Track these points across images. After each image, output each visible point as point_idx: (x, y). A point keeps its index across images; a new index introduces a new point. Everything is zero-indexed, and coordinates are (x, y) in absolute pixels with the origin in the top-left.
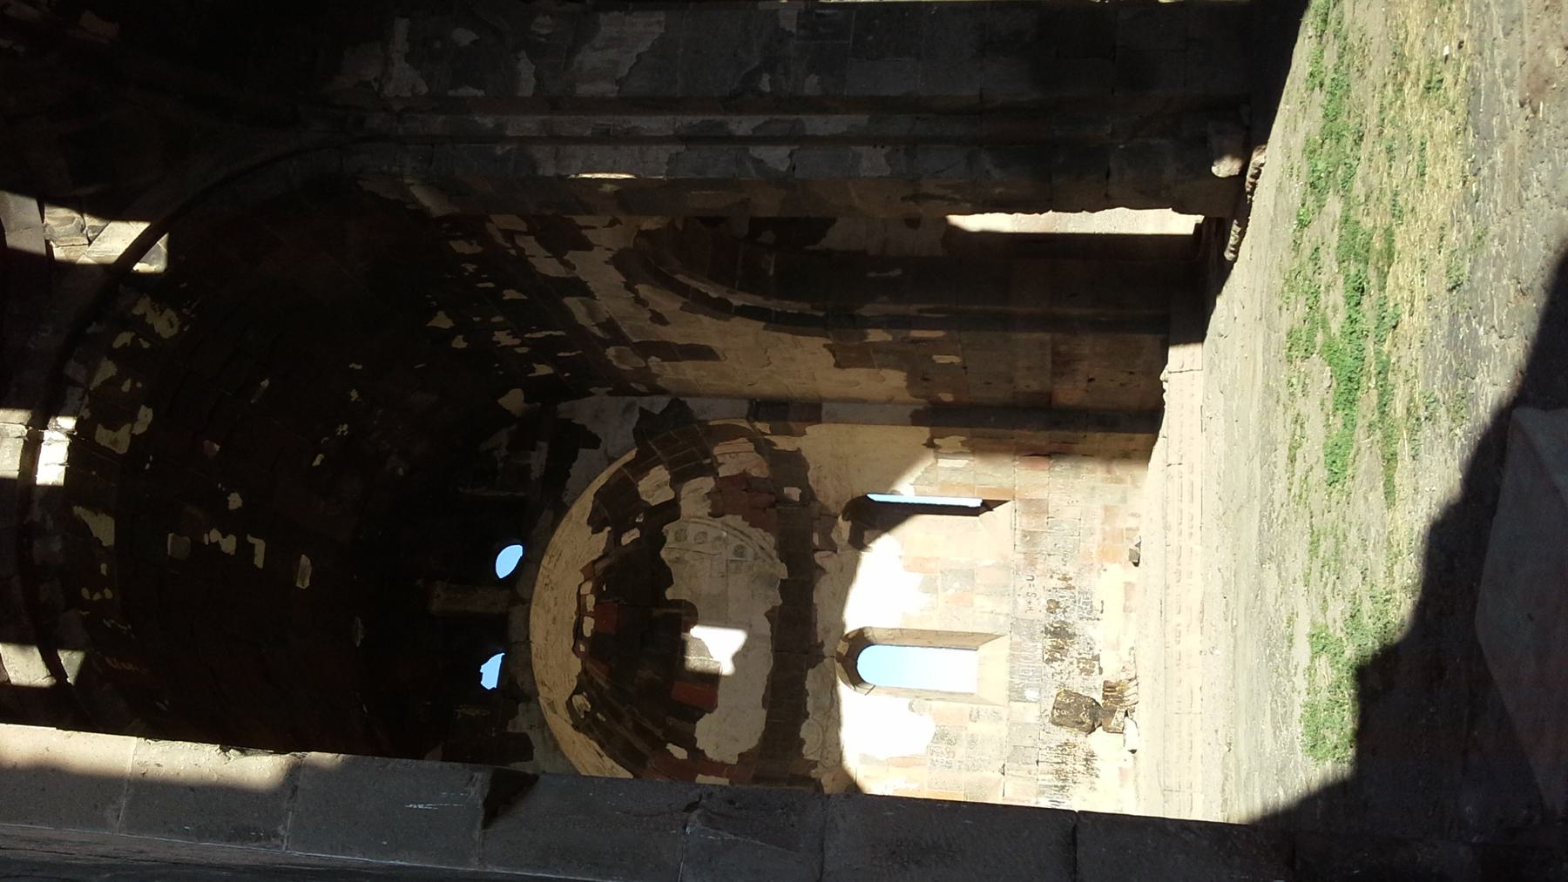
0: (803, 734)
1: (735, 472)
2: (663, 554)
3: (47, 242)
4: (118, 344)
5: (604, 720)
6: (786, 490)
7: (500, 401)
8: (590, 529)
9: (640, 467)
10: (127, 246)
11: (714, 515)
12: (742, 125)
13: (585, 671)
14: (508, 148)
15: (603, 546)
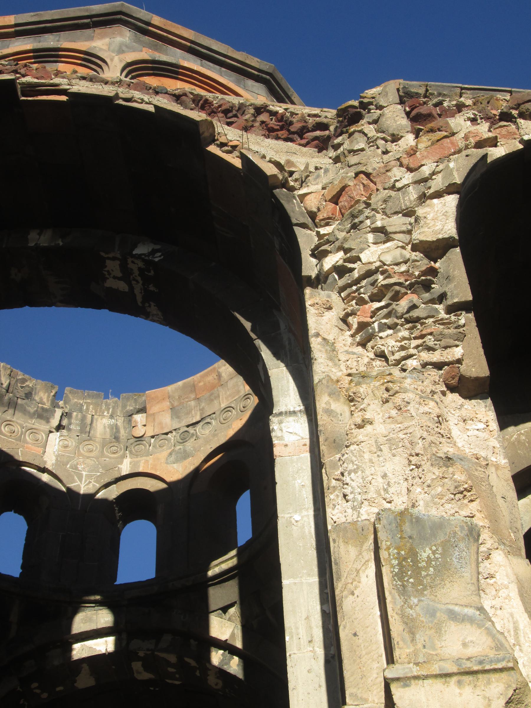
4: (186, 659)
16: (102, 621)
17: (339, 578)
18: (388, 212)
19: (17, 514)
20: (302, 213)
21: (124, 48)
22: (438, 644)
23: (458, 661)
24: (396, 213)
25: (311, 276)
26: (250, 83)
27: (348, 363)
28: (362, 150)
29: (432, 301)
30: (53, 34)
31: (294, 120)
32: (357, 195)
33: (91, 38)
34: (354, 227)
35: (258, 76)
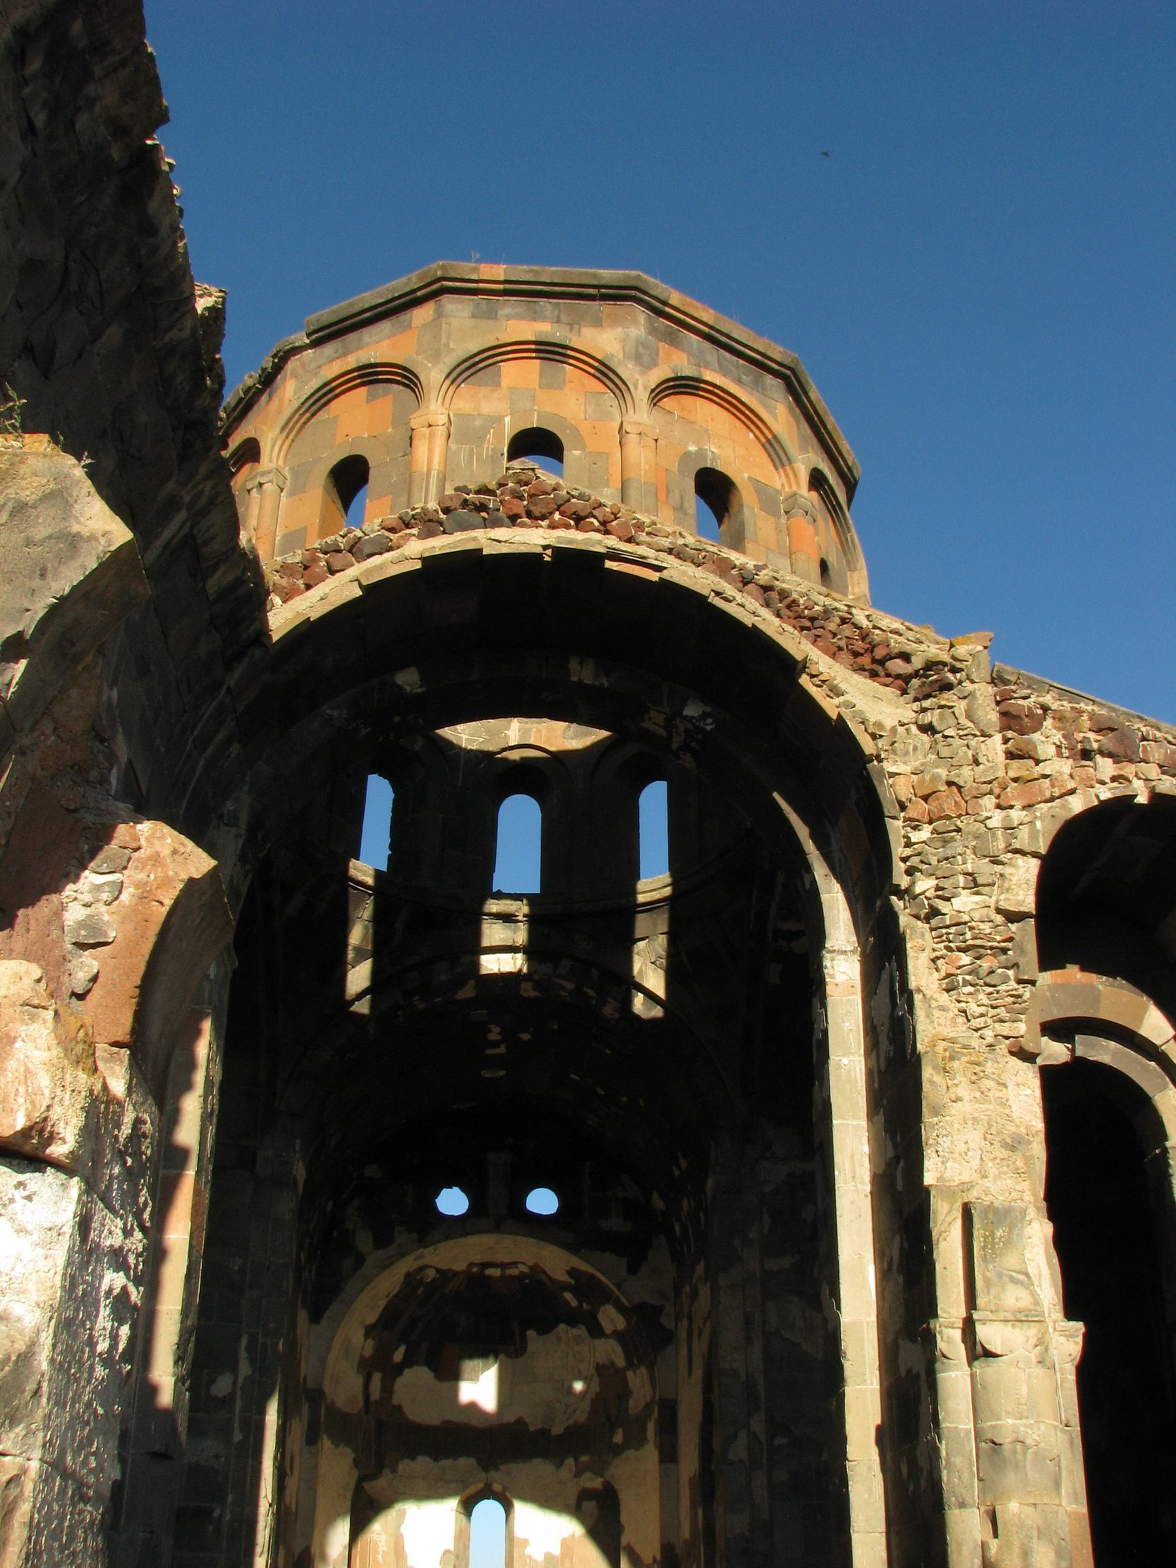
0: (420, 1459)
1: (630, 1385)
2: (562, 1327)
3: (647, 937)
4: (585, 989)
5: (419, 1293)
6: (620, 1431)
7: (656, 1195)
8: (568, 1268)
9: (621, 1308)
10: (651, 989)
11: (599, 1369)
12: (757, 1424)
13: (456, 1274)
14: (739, 1249)
15: (561, 1279)
16: (497, 937)
17: (935, 1222)
18: (978, 853)
19: (381, 778)
20: (892, 800)
21: (641, 350)
22: (1002, 1297)
23: (1014, 1313)
24: (986, 856)
25: (899, 885)
26: (769, 379)
27: (940, 1020)
28: (952, 737)
29: (1007, 968)
30: (551, 300)
31: (877, 639)
32: (948, 809)
33: (598, 323)
34: (947, 859)
35: (778, 371)
